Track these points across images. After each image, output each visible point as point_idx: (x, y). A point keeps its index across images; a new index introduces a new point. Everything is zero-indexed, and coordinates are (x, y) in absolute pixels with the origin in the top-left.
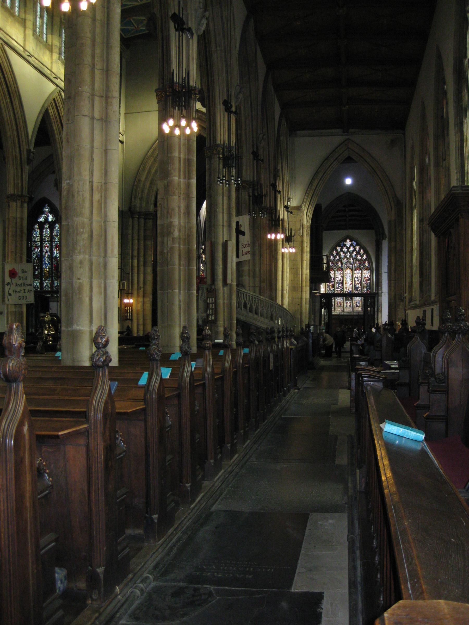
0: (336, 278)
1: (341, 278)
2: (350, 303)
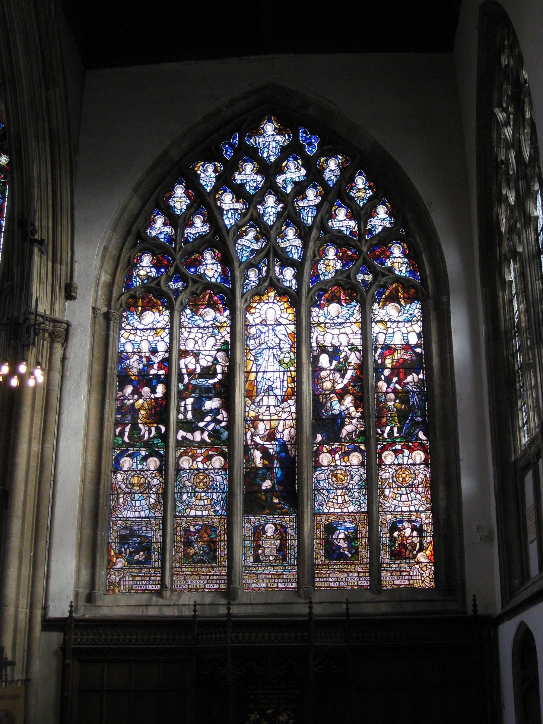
0: (184, 354)
2: (281, 530)
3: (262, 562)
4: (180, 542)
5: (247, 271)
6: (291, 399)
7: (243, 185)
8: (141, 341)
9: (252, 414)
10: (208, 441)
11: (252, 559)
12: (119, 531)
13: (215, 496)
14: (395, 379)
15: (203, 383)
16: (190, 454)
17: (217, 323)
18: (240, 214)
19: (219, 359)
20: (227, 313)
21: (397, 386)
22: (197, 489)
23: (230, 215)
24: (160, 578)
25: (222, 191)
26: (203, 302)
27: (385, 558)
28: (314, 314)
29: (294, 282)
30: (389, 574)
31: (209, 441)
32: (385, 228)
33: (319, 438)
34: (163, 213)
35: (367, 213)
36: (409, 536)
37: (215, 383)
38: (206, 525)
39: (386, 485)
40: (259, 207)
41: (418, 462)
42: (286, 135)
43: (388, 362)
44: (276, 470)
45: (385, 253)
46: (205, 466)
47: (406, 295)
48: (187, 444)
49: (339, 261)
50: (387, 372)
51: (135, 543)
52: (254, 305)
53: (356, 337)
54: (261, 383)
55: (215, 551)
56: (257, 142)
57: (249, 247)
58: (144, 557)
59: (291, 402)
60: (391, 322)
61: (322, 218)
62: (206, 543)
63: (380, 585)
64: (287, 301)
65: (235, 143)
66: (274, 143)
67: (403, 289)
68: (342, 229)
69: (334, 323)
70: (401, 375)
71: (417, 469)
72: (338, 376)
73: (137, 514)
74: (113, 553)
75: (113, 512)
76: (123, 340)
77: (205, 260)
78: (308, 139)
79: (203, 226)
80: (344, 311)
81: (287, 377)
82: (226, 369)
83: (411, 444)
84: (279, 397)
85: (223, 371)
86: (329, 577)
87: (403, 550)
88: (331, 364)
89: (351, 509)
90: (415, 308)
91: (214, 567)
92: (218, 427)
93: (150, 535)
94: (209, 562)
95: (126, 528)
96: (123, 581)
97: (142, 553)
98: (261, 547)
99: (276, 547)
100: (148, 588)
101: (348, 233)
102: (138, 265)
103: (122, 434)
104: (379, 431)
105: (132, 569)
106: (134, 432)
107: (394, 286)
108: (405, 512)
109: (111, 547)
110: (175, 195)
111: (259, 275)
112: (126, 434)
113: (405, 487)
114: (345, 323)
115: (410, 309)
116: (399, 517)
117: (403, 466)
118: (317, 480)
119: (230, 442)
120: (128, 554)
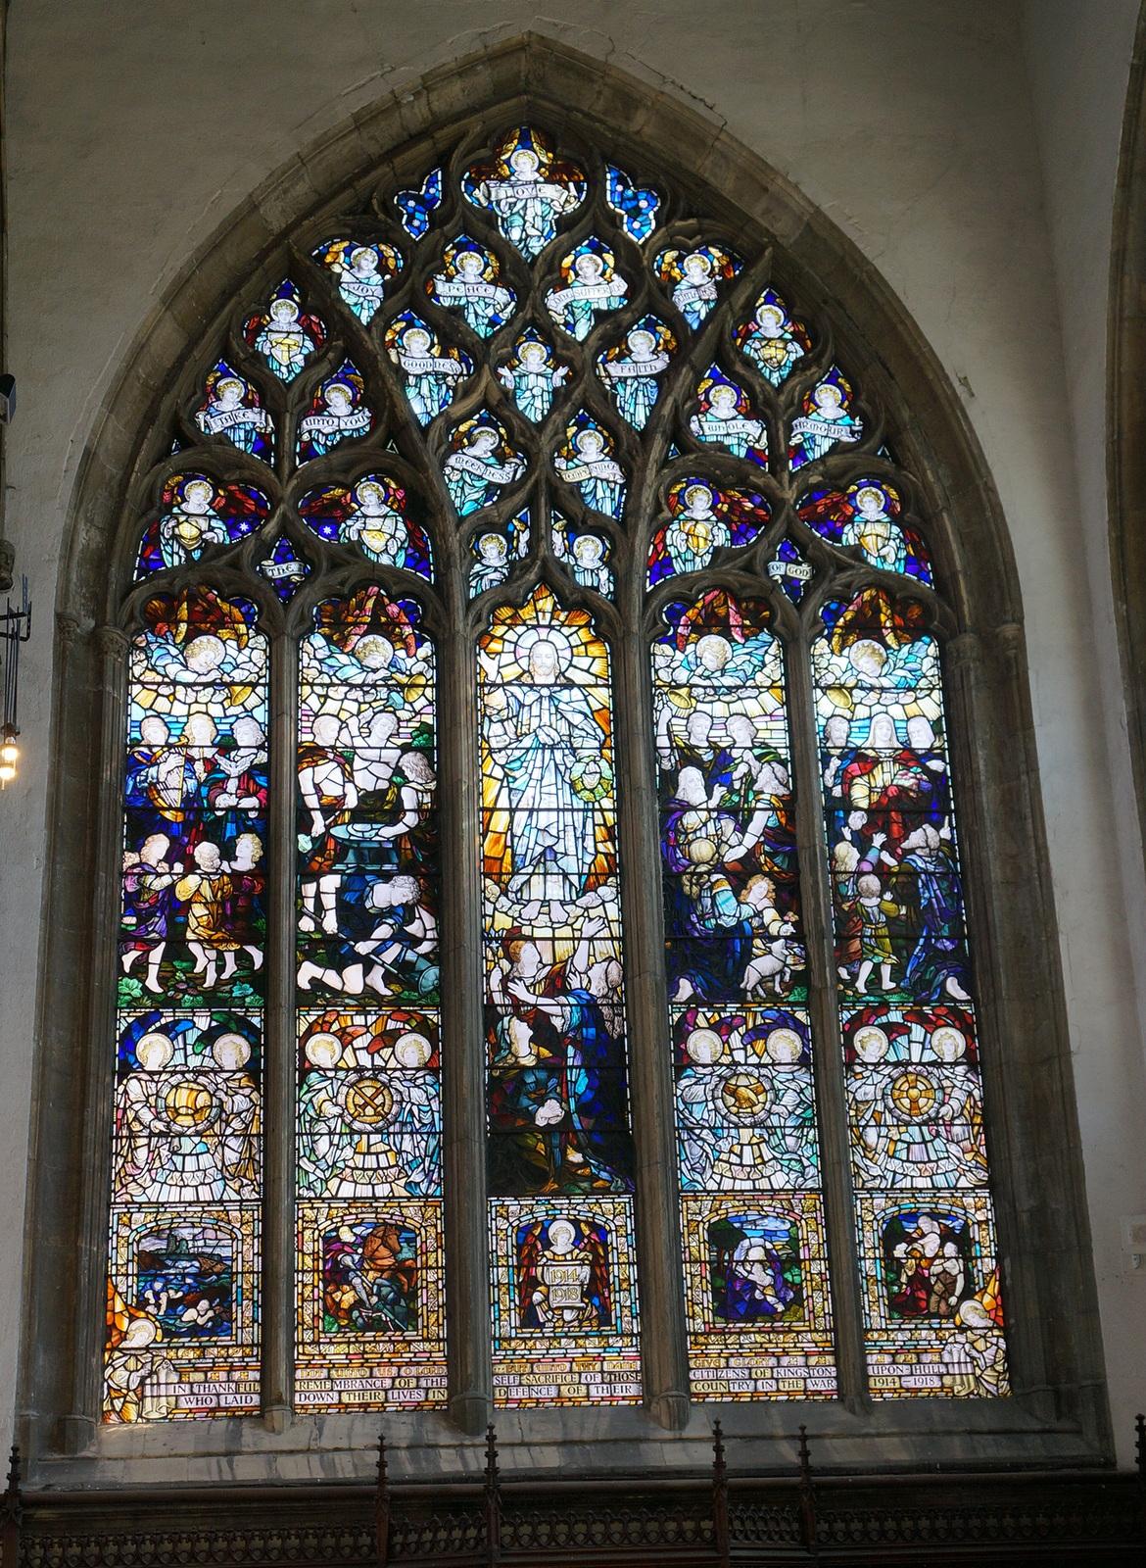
0: (314, 754)
1: (412, 763)
2: (593, 1240)
3: (542, 1326)
4: (314, 1270)
5: (478, 540)
6: (605, 884)
7: (457, 312)
8: (189, 715)
9: (503, 922)
10: (384, 991)
11: (515, 1320)
12: (138, 1242)
13: (407, 1145)
14: (879, 839)
15: (367, 835)
16: (335, 1027)
17: (398, 676)
18: (455, 390)
19: (407, 773)
20: (426, 649)
21: (886, 857)
22: (357, 1125)
23: (425, 391)
24: (257, 1375)
25: (403, 324)
26: (358, 616)
27: (876, 1316)
28: (660, 662)
29: (604, 574)
30: (887, 1359)
31: (389, 993)
32: (837, 447)
33: (686, 989)
34: (241, 373)
35: (792, 404)
36: (937, 1256)
37: (399, 837)
38: (385, 1224)
39: (867, 1117)
40: (504, 371)
41: (949, 1059)
42: (571, 185)
43: (859, 793)
44: (572, 1075)
45: (840, 510)
46: (379, 1062)
47: (899, 621)
48: (326, 999)
49: (721, 525)
50: (857, 820)
51: (184, 1276)
52: (499, 630)
53: (772, 725)
54: (524, 840)
55: (413, 1296)
56: (493, 198)
57: (481, 478)
58: (210, 1314)
59: (607, 892)
60: (862, 688)
61: (676, 408)
62: (385, 1275)
63: (867, 1388)
64: (588, 625)
65: (434, 199)
66: (537, 203)
67: (892, 603)
68: (727, 441)
69: (713, 687)
70: (895, 827)
71: (947, 1078)
72: (728, 825)
73: (189, 1195)
74: (119, 1306)
75: (118, 1186)
76: (137, 713)
77: (361, 505)
78: (629, 199)
79: (352, 414)
80: (741, 657)
81: (594, 825)
82: (427, 799)
83: (927, 1010)
84: (574, 879)
85: (420, 804)
86: (728, 1367)
87: (922, 1295)
88: (710, 795)
89: (779, 1181)
90: (924, 655)
91: (409, 1343)
92: (410, 956)
93: (226, 1252)
94: (397, 1328)
95: (156, 1233)
96: (152, 1385)
97: (204, 1304)
98: (540, 1284)
99: (582, 1285)
100: (223, 1404)
101: (743, 453)
102: (175, 510)
103: (140, 969)
104: (844, 973)
105: (178, 1348)
106: (176, 963)
107: (866, 595)
108: (921, 1190)
109: (116, 1287)
110: (272, 326)
111: (509, 552)
112: (153, 970)
113: (919, 1125)
114: (744, 686)
115: (912, 658)
116: (907, 1205)
117: (910, 1069)
118: (684, 1103)
119: (442, 994)
120: (163, 1308)
